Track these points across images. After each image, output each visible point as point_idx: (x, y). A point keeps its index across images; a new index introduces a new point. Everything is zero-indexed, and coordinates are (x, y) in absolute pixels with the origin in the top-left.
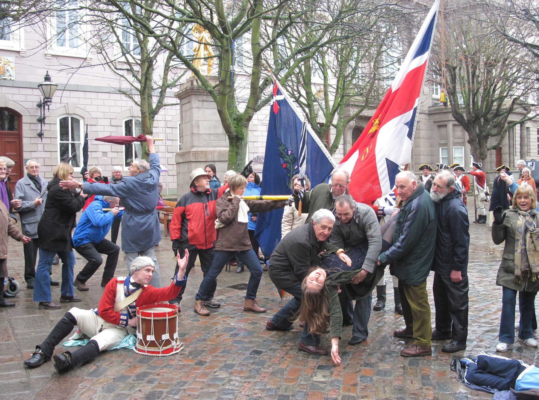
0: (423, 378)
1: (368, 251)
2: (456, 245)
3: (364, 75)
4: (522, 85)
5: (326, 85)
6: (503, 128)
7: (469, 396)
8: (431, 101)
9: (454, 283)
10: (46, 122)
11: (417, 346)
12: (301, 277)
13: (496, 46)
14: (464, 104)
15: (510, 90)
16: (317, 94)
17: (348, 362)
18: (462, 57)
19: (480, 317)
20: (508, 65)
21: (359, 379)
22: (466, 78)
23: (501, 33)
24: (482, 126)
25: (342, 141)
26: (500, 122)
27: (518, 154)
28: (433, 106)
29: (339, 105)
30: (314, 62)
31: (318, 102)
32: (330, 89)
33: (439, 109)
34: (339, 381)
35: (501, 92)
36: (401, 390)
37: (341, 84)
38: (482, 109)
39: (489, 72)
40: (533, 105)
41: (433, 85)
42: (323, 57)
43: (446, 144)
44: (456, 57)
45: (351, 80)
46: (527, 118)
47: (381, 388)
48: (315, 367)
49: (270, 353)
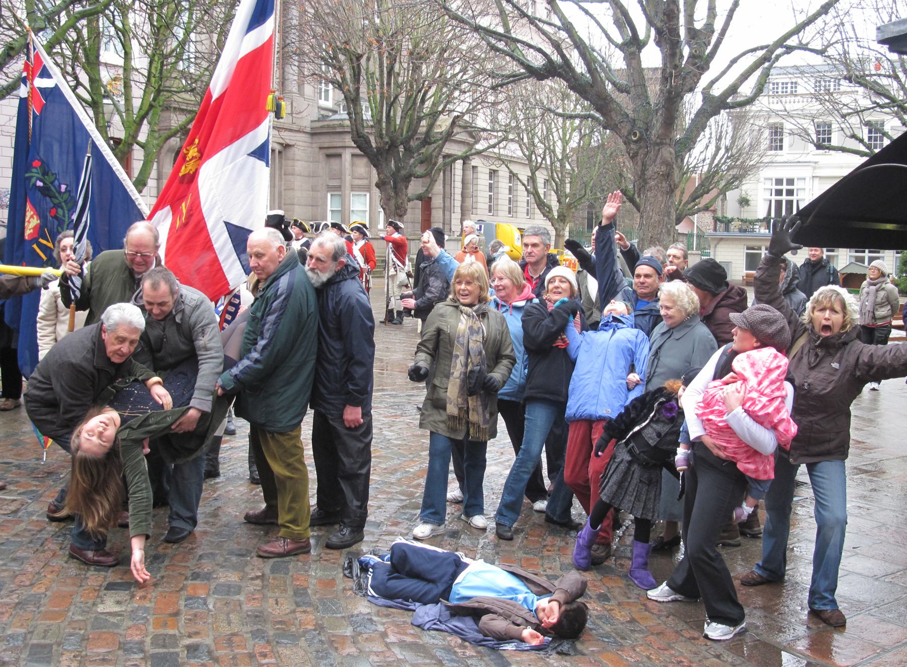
0: (296, 593)
1: (199, 374)
2: (352, 362)
3: (200, 55)
4: (468, 94)
5: (127, 68)
6: (435, 164)
7: (375, 618)
8: (316, 110)
9: (349, 429)
11: (284, 539)
12: (73, 422)
13: (429, 25)
14: (373, 120)
15: (448, 102)
16: (111, 84)
17: (162, 573)
18: (373, 39)
19: (392, 484)
20: (448, 59)
21: (182, 603)
22: (377, 75)
23: (439, 5)
24: (400, 159)
25: (154, 174)
26: (431, 155)
27: (458, 210)
28: (319, 121)
29: (151, 106)
30: (107, 23)
31: (112, 100)
32: (135, 76)
33: (328, 127)
34: (147, 610)
35: (434, 104)
36: (258, 617)
37: (156, 68)
38: (402, 130)
39: (416, 69)
40: (484, 130)
41: (321, 83)
42: (124, 16)
43: (339, 188)
44: (363, 38)
45: (176, 63)
46: (473, 151)
47: (223, 617)
48: (101, 586)
49: (15, 567)
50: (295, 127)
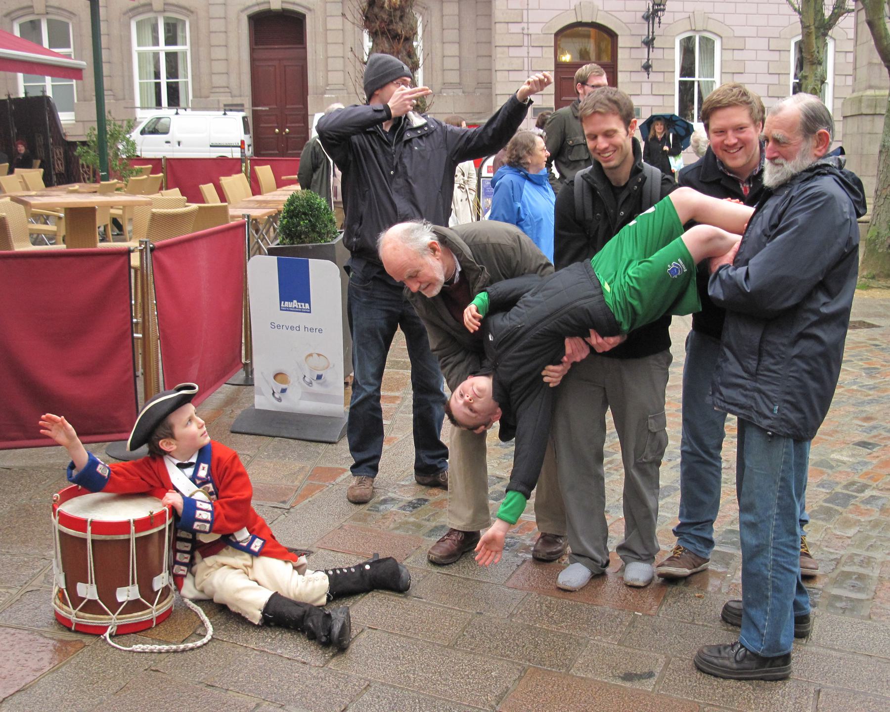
10: (655, 45)
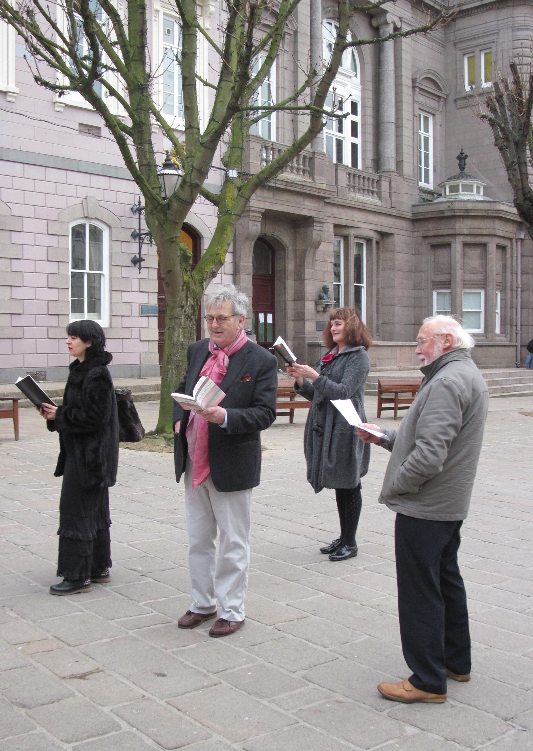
8: (417, 192)
43: (447, 284)
50: (394, 212)
